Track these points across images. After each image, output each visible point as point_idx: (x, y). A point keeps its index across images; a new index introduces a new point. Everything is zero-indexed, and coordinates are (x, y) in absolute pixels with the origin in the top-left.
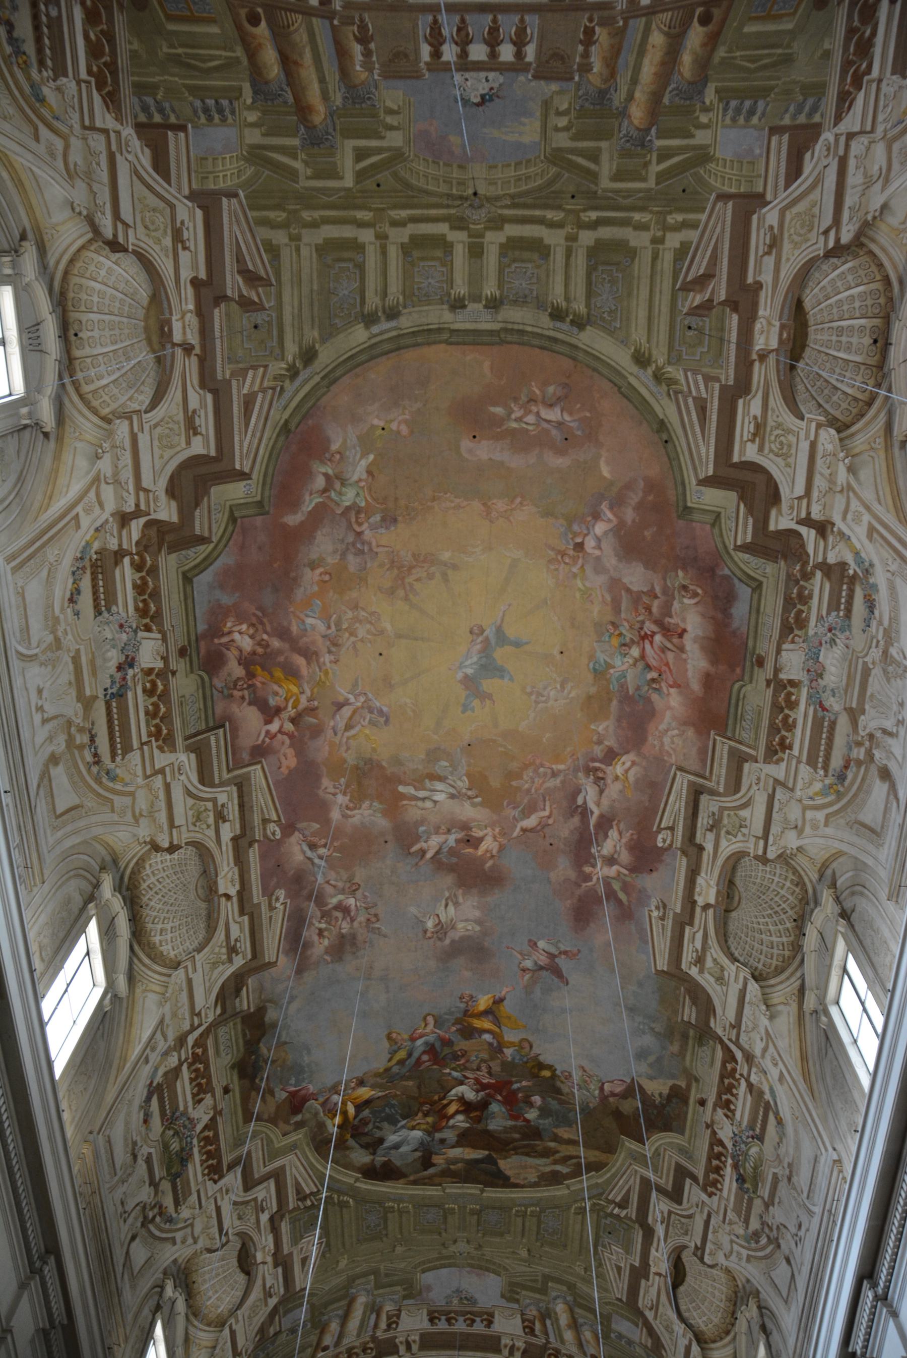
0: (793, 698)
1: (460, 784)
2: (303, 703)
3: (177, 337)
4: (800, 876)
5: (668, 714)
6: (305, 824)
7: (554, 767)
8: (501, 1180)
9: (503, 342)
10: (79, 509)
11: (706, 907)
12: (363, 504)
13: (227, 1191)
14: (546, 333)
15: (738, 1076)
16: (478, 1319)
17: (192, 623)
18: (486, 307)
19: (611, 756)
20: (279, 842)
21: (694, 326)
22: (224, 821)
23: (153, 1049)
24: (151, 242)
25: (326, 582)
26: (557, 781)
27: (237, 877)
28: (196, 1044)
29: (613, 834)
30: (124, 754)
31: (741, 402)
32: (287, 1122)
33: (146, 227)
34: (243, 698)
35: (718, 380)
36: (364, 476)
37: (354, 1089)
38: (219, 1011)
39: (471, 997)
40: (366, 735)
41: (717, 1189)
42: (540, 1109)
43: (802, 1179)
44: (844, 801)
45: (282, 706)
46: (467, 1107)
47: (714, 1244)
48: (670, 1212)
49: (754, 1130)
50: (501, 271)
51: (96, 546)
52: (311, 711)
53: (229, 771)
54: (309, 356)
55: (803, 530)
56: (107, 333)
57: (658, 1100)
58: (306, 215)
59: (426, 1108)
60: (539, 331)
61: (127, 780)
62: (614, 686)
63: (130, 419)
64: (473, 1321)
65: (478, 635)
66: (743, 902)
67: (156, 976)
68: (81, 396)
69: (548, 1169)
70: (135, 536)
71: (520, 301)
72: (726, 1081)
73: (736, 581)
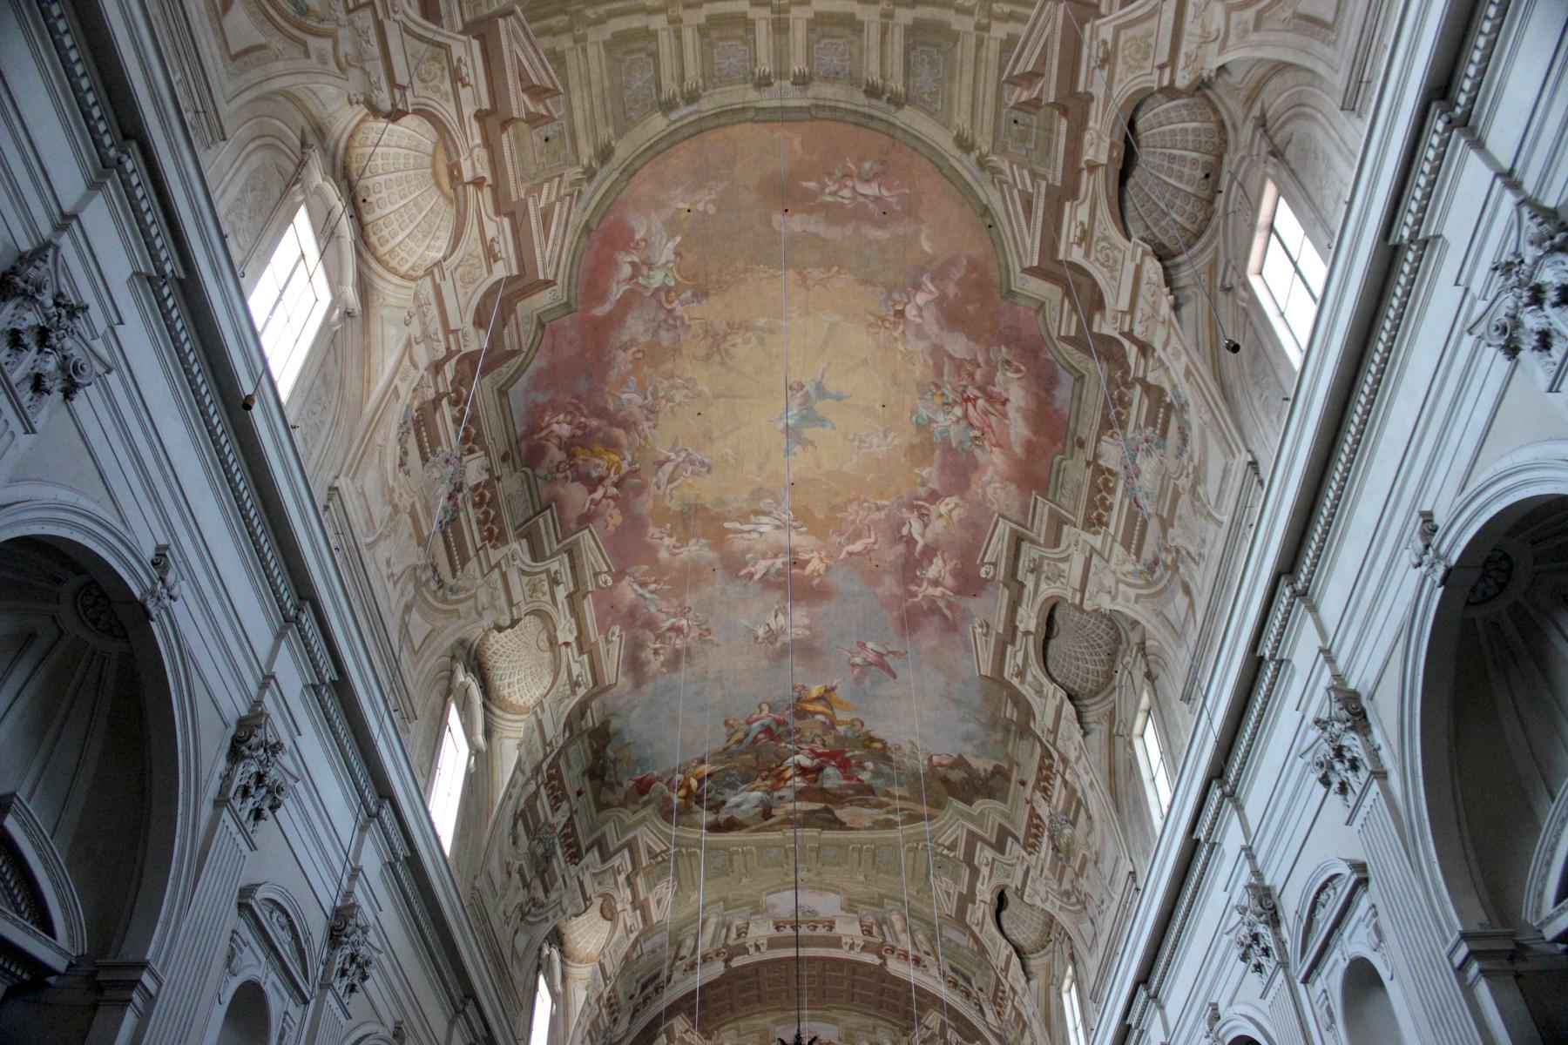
1: (785, 517)
2: (625, 467)
3: (468, 175)
5: (991, 468)
6: (635, 568)
9: (813, 119)
10: (397, 381)
11: (1027, 633)
12: (672, 284)
17: (511, 430)
18: (794, 83)
19: (934, 497)
21: (1020, 120)
22: (558, 584)
23: (514, 787)
24: (429, 93)
26: (882, 514)
27: (574, 626)
28: (550, 767)
29: (938, 561)
30: (463, 564)
31: (1068, 205)
32: (635, 802)
33: (423, 81)
34: (566, 477)
35: (1045, 178)
36: (672, 257)
38: (567, 735)
40: (690, 485)
42: (872, 772)
43: (1106, 867)
45: (605, 474)
46: (803, 771)
48: (994, 860)
50: (809, 49)
51: (416, 404)
52: (633, 473)
53: (558, 542)
54: (605, 154)
55: (1126, 343)
56: (395, 190)
57: (983, 774)
58: (590, 13)
59: (764, 774)
60: (854, 108)
61: (468, 585)
62: (937, 438)
63: (432, 273)
64: (815, 927)
66: (1062, 634)
68: (379, 260)
69: (881, 817)
70: (449, 376)
71: (832, 78)
72: (1044, 772)
73: (1059, 367)
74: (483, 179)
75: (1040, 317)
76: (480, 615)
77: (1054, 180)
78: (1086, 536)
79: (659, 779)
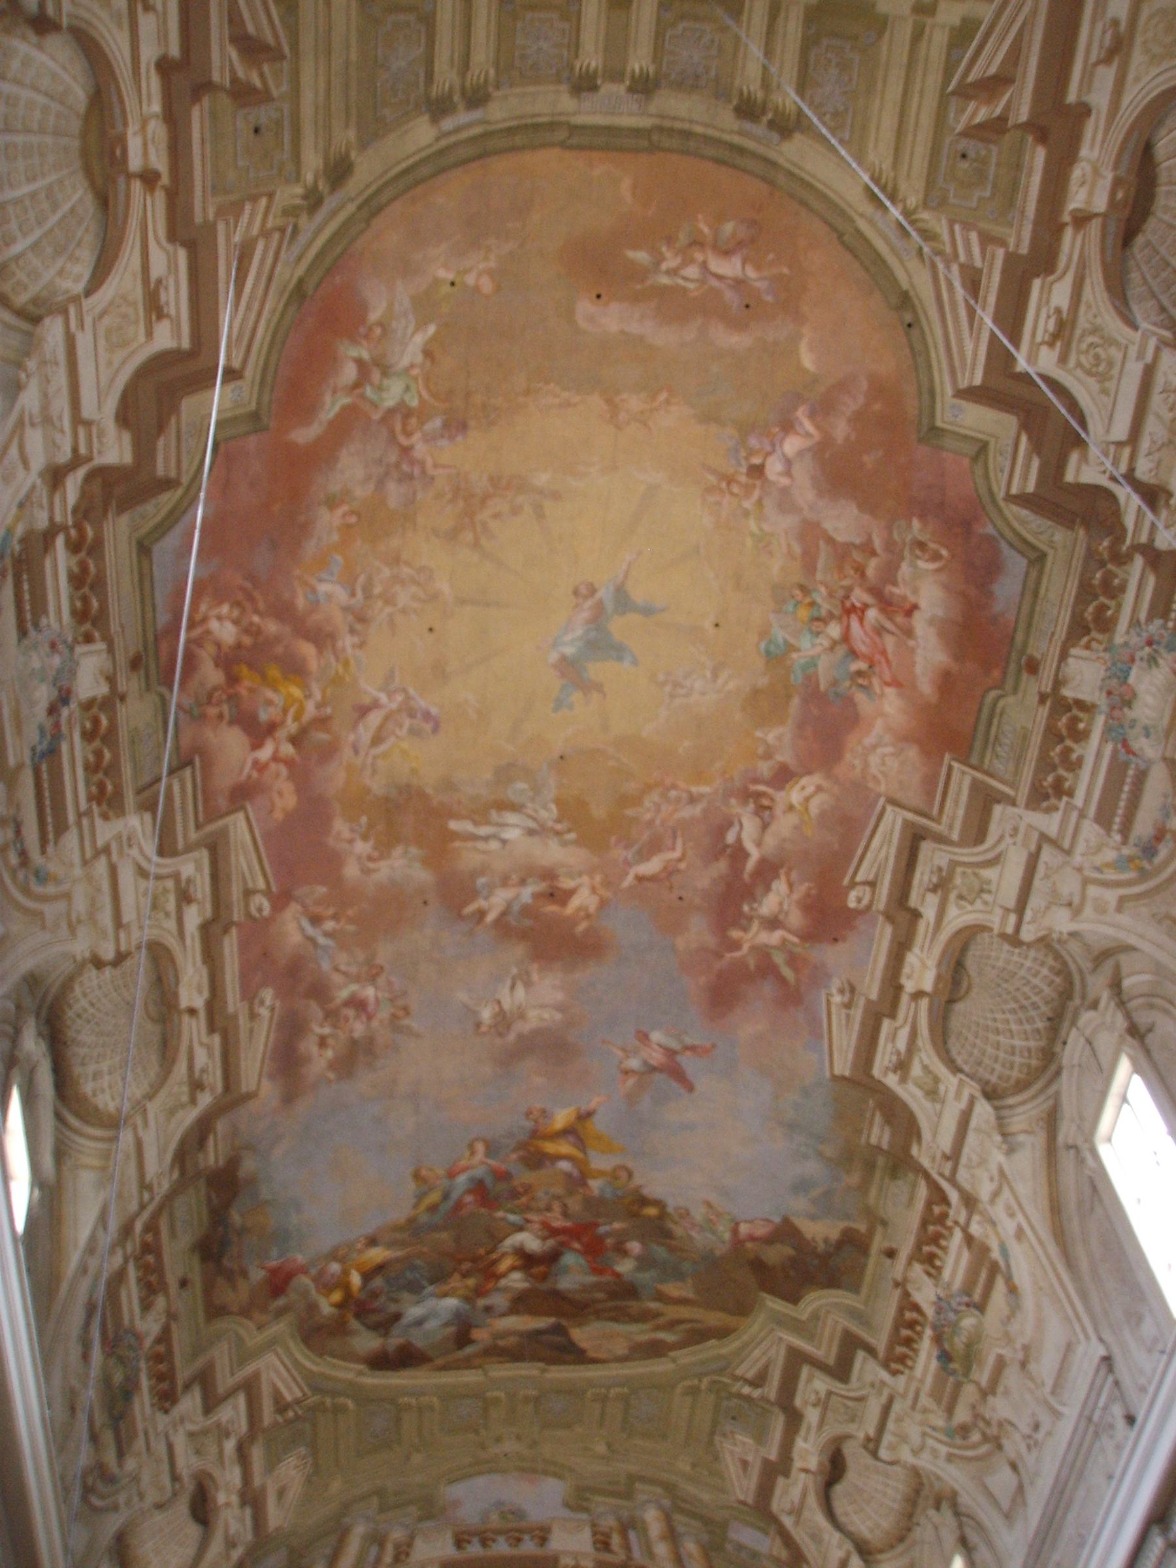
0: (1081, 726)
1: (543, 814)
2: (310, 710)
3: (135, 163)
4: (1065, 963)
5: (879, 724)
7: (694, 789)
8: (576, 1355)
9: (653, 149)
11: (918, 995)
12: (414, 403)
13: (182, 1420)
14: (726, 137)
15: (949, 1223)
16: (526, 1537)
17: (149, 615)
18: (630, 90)
19: (784, 777)
20: (267, 921)
21: (972, 154)
25: (349, 526)
26: (697, 810)
29: (780, 886)
31: (1037, 283)
35: (1003, 243)
36: (420, 358)
37: (360, 1252)
38: (176, 1175)
39: (544, 1111)
41: (906, 1366)
42: (639, 1259)
43: (1046, 1366)
44: (1151, 884)
46: (527, 1260)
47: (895, 1434)
48: (830, 1393)
49: (969, 1295)
50: (659, 35)
51: (19, 531)
52: (322, 722)
53: (198, 827)
57: (821, 1247)
59: (466, 1266)
60: (716, 134)
62: (797, 678)
63: (65, 312)
64: (519, 1540)
65: (586, 598)
66: (975, 990)
67: (92, 1144)
71: (688, 83)
74: (157, 175)
75: (979, 471)
76: (72, 929)
77: (1017, 245)
78: (1036, 819)
79: (304, 1270)
